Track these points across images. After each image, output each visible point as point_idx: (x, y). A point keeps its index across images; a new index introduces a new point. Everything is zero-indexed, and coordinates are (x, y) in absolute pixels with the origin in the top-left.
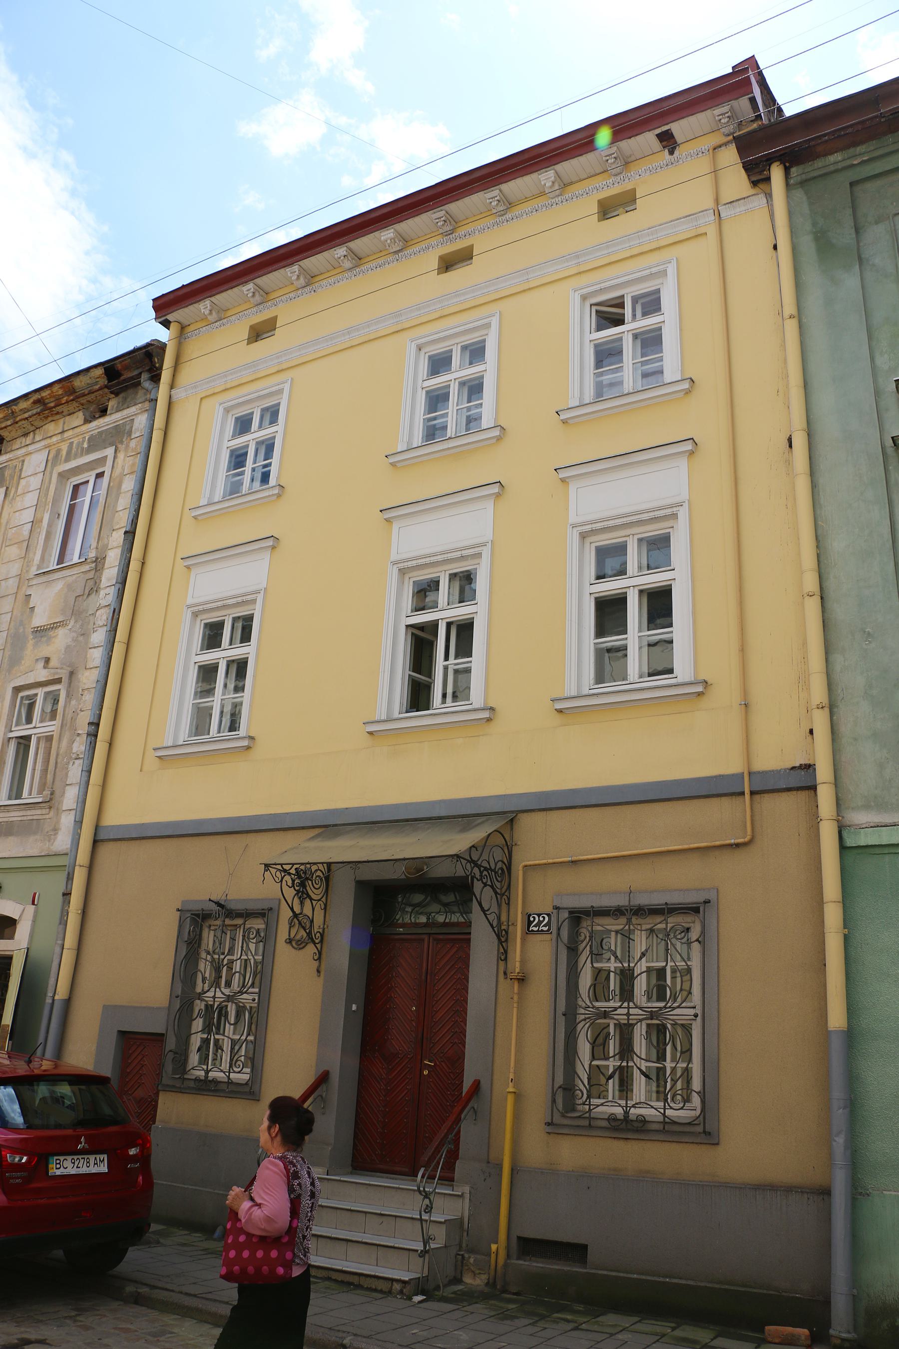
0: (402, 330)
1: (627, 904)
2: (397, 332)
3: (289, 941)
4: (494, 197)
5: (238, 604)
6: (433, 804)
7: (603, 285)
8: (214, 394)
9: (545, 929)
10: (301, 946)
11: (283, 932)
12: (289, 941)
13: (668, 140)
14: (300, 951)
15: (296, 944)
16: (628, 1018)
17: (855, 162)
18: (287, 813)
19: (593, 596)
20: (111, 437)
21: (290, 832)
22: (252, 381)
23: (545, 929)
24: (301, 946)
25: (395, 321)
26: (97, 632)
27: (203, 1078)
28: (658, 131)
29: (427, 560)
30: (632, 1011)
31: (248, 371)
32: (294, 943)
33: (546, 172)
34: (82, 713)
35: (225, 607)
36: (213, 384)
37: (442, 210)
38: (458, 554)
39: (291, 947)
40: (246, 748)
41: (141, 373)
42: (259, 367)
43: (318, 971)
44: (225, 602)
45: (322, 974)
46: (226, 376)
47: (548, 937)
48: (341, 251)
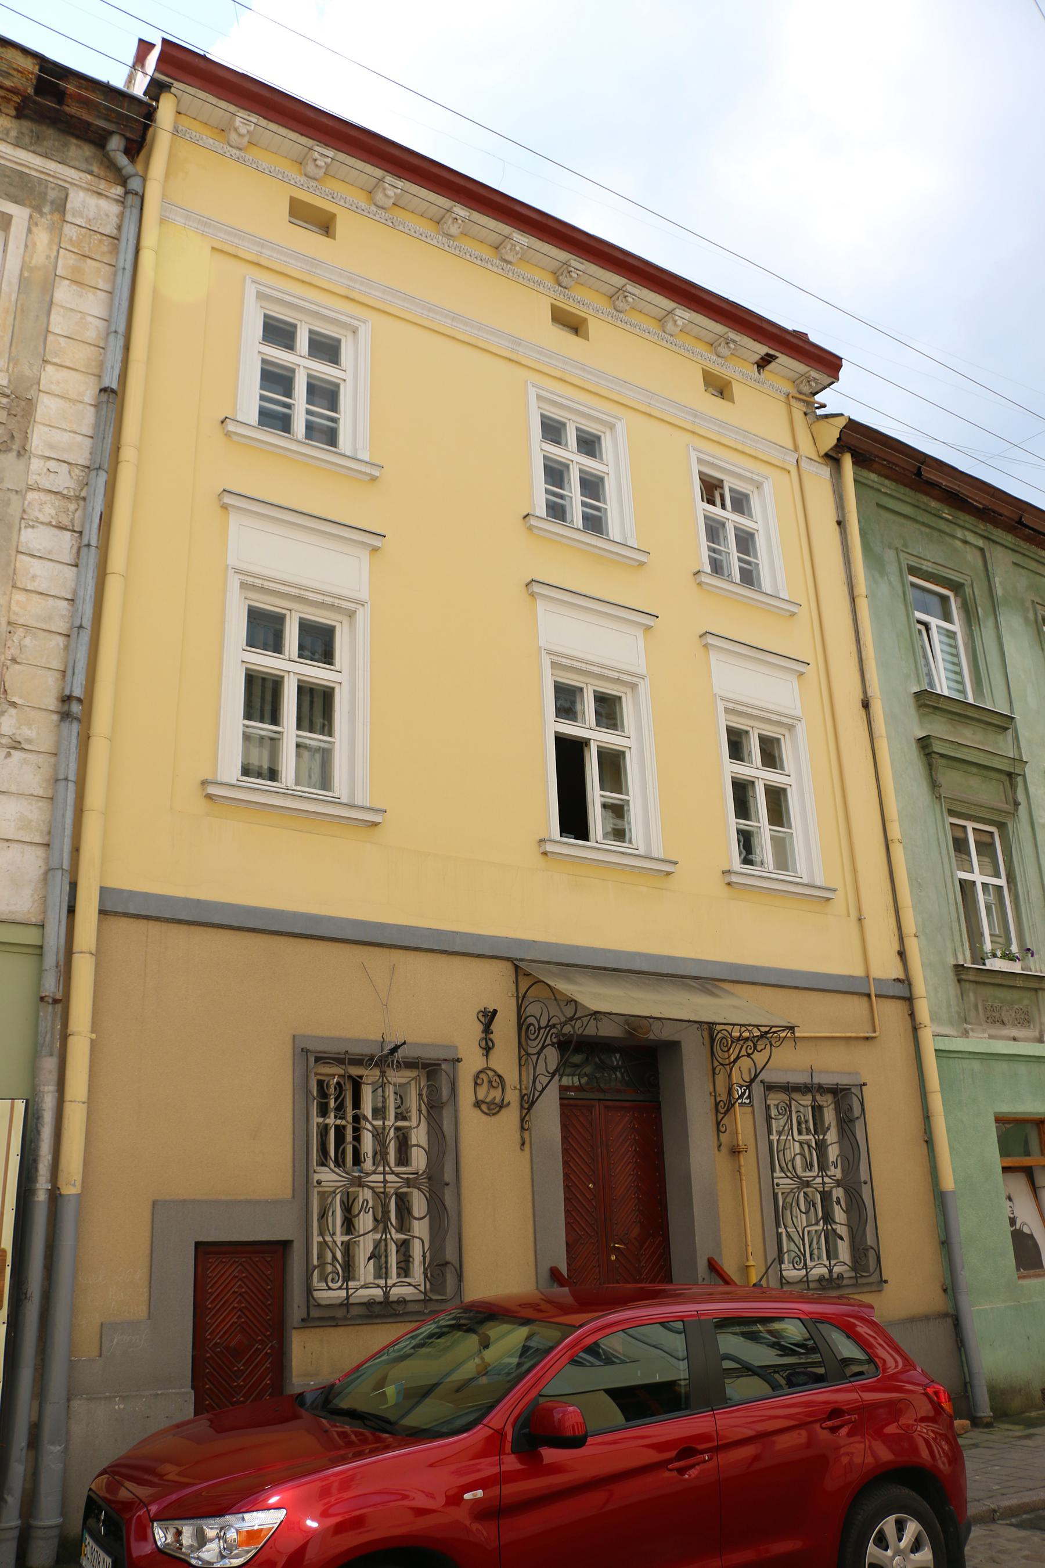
0: (517, 362)
1: (810, 1082)
2: (510, 360)
3: (478, 1104)
4: (577, 270)
5: (322, 605)
6: (617, 954)
7: (716, 461)
8: (236, 256)
9: (747, 1101)
10: (494, 1111)
11: (466, 1094)
12: (478, 1104)
13: (764, 362)
14: (493, 1118)
15: (489, 1109)
16: (385, 1185)
17: (883, 490)
18: (457, 933)
19: (245, 665)
20: (11, 185)
21: (457, 961)
22: (303, 282)
23: (747, 1101)
24: (494, 1111)
25: (510, 345)
26: (35, 530)
27: (382, 1299)
28: (772, 352)
29: (584, 666)
30: (389, 1178)
31: (299, 264)
32: (484, 1107)
33: (684, 310)
34: (17, 667)
35: (299, 599)
36: (236, 241)
37: (582, 264)
38: (616, 675)
39: (479, 1111)
40: (370, 824)
41: (114, 132)
42: (318, 272)
43: (523, 1144)
44: (302, 592)
45: (527, 1146)
46: (263, 246)
47: (750, 1109)
48: (460, 211)
